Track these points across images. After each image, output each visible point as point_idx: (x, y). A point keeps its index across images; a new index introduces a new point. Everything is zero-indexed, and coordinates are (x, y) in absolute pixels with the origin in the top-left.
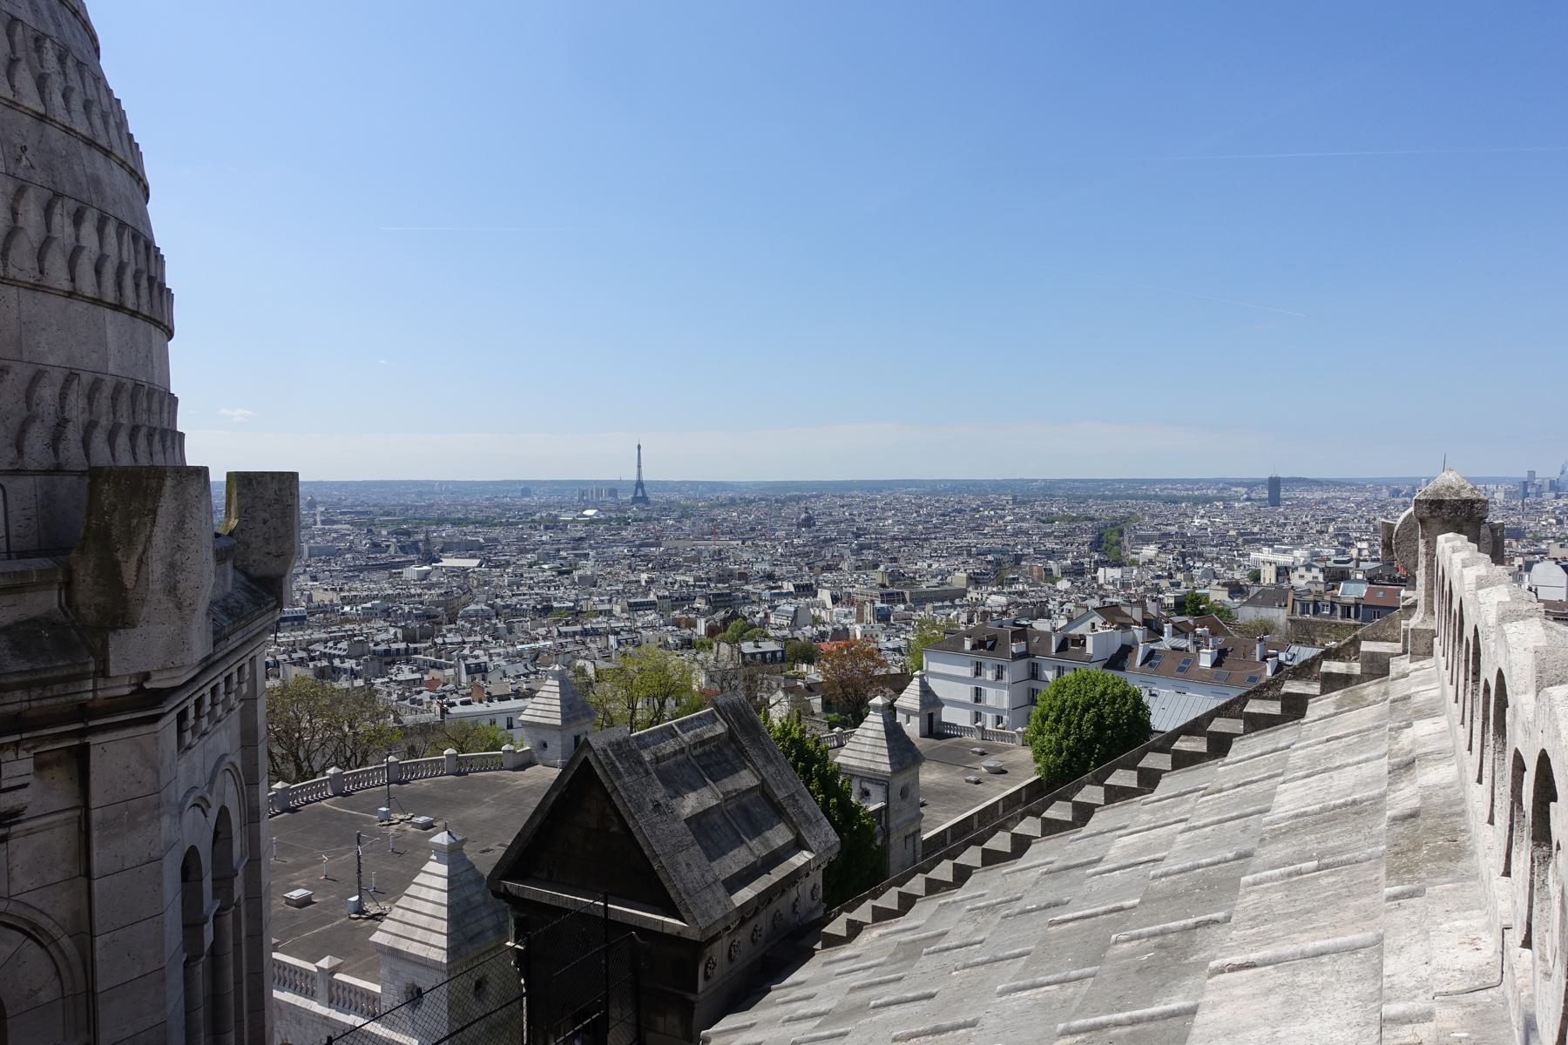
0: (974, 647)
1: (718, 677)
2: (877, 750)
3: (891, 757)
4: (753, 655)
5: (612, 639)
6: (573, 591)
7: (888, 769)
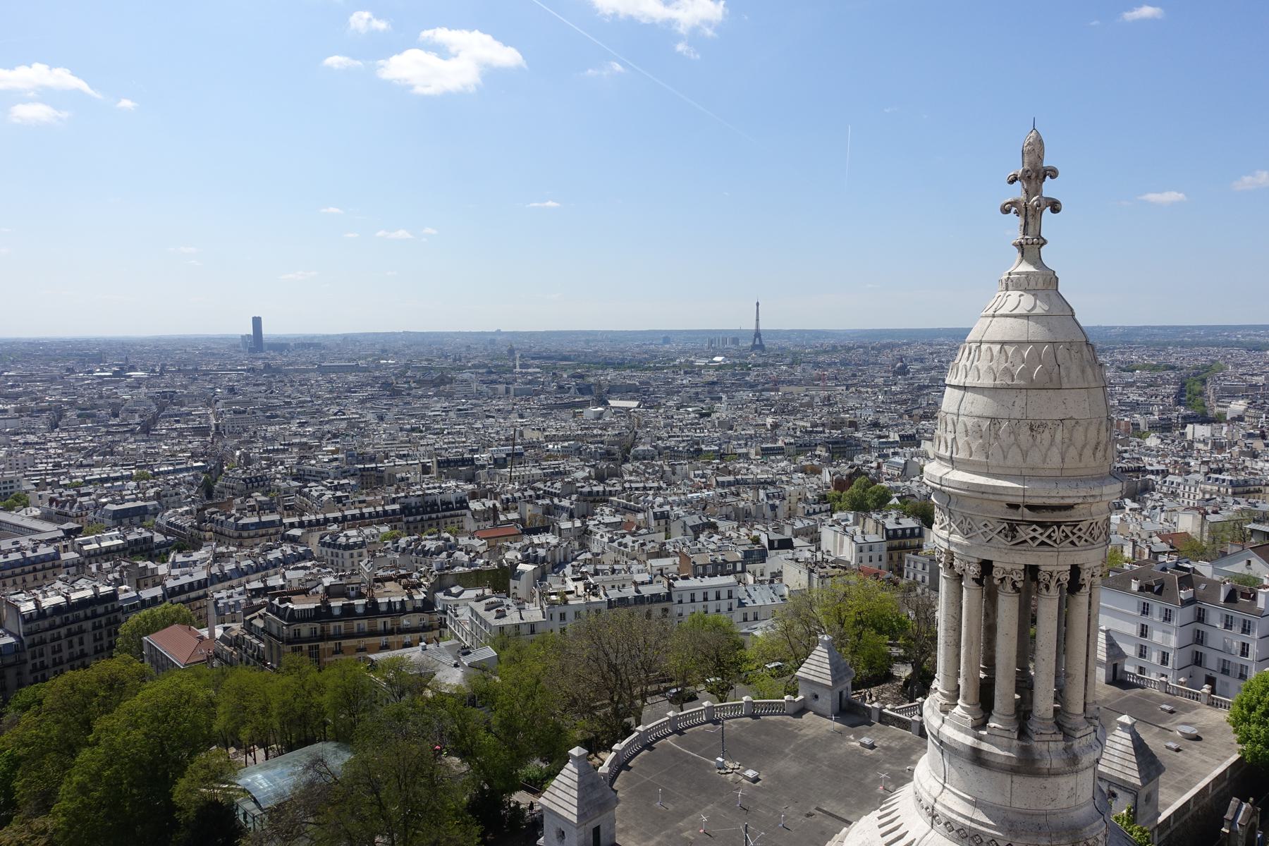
0: (1141, 589)
1: (866, 548)
2: (1126, 763)
3: (1140, 772)
4: (895, 531)
5: (762, 493)
6: (716, 435)
7: (1139, 783)
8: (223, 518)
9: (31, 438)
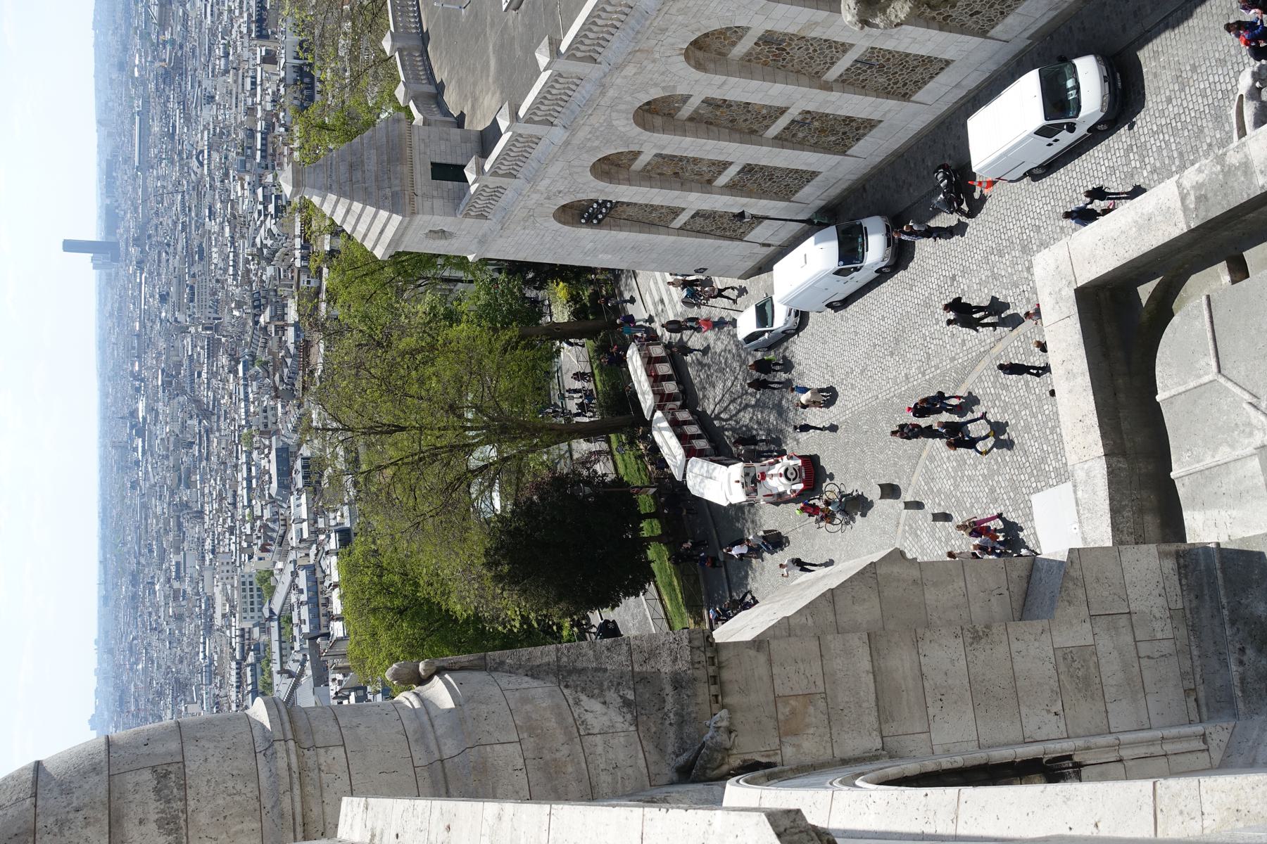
8: (286, 370)
9: (208, 545)
